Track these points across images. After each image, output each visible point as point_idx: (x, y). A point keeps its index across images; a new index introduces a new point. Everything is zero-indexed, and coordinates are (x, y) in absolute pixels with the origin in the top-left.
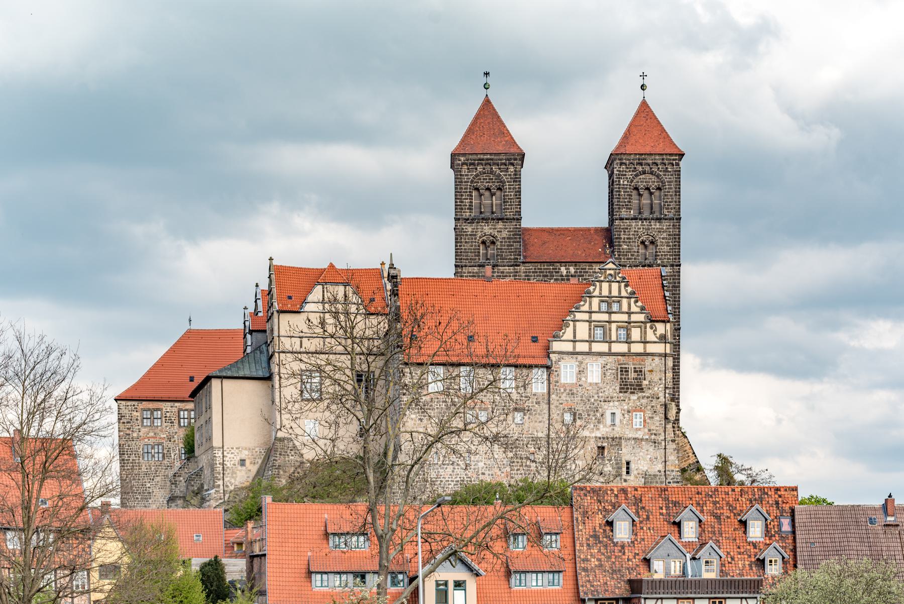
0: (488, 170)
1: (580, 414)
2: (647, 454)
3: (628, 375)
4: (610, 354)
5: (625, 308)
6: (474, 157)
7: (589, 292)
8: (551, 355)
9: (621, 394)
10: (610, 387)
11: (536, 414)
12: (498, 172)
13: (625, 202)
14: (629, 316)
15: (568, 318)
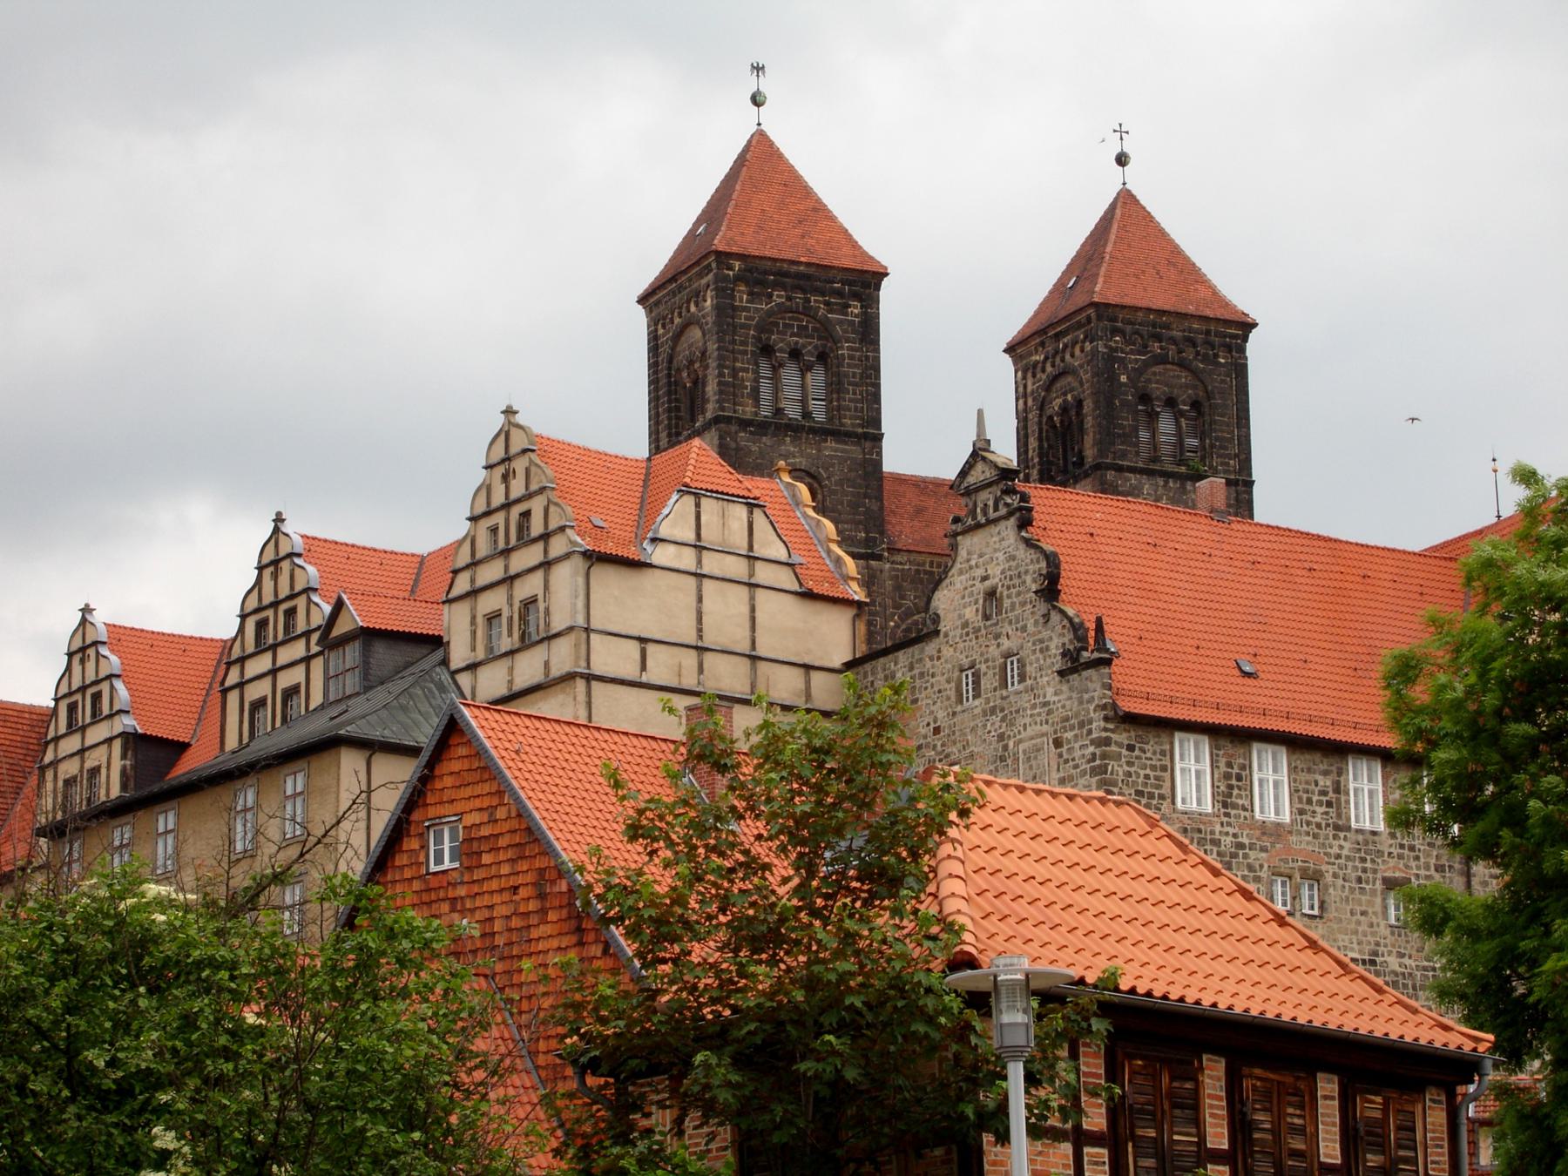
0: (797, 303)
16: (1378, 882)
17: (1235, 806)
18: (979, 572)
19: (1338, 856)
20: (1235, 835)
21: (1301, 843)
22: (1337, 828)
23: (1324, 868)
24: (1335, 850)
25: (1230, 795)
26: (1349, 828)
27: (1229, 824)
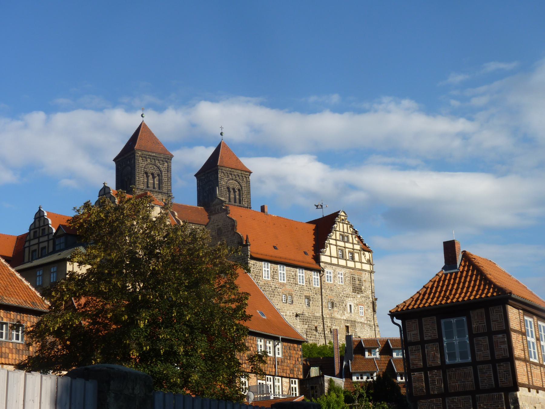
1: (336, 304)
2: (367, 333)
3: (355, 282)
4: (346, 267)
5: (351, 241)
6: (146, 153)
7: (335, 228)
8: (321, 264)
9: (353, 293)
10: (348, 288)
11: (315, 301)
12: (159, 164)
13: (224, 194)
14: (353, 246)
15: (326, 242)
16: (304, 296)
17: (275, 279)
18: (216, 224)
19: (296, 290)
20: (275, 285)
21: (288, 287)
22: (296, 284)
23: (293, 293)
24: (295, 289)
25: (274, 276)
26: (298, 284)
27: (274, 283)
